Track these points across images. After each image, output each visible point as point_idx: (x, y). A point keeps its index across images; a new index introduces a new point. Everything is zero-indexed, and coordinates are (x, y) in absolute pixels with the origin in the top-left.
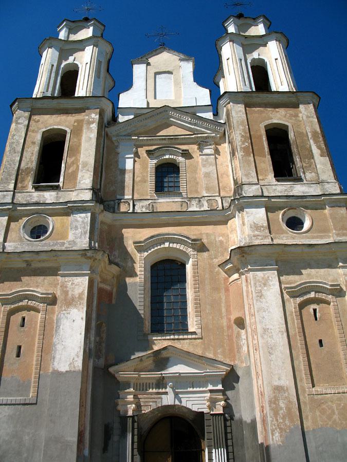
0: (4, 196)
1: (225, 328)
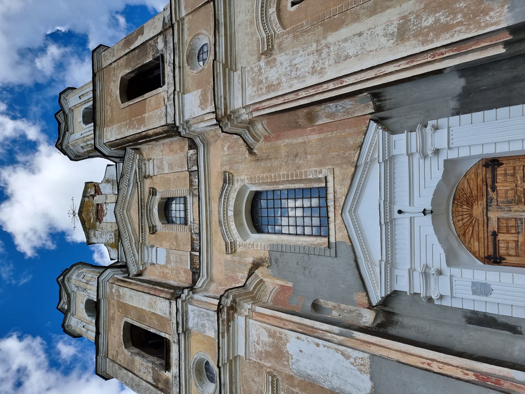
1: (322, 136)
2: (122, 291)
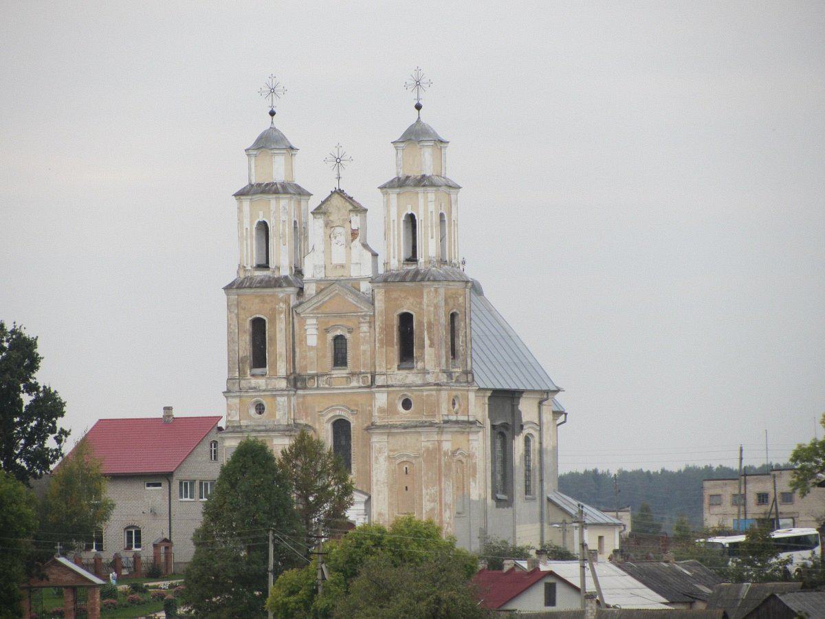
0: (234, 384)
2: (282, 316)
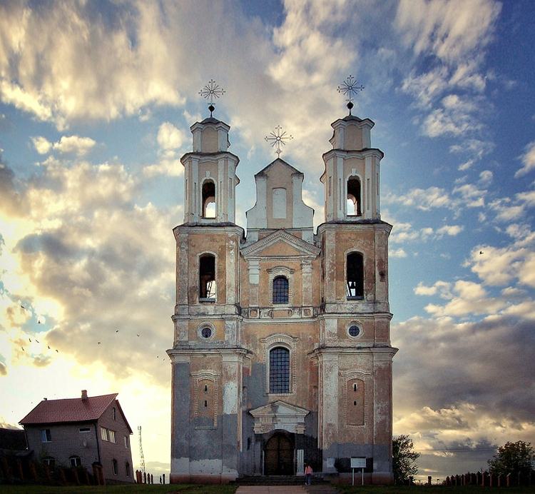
0: (184, 309)
